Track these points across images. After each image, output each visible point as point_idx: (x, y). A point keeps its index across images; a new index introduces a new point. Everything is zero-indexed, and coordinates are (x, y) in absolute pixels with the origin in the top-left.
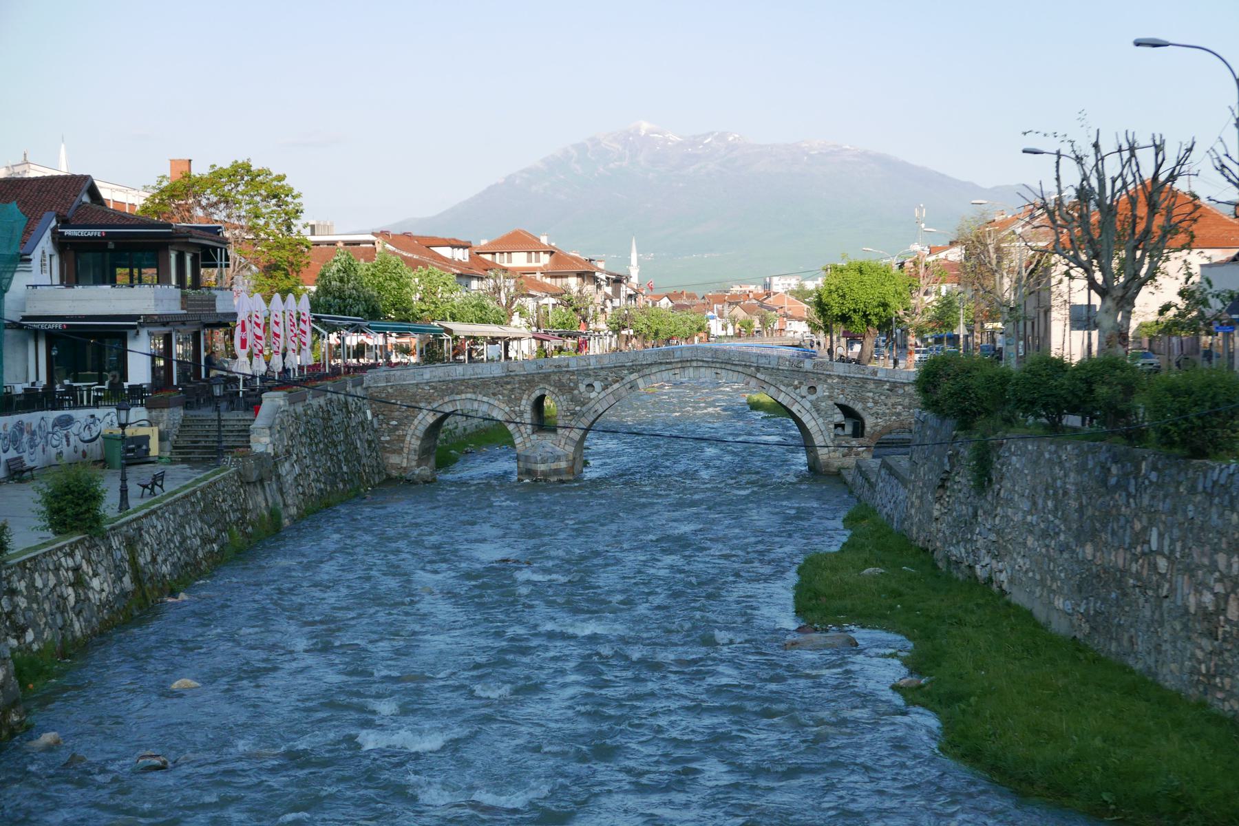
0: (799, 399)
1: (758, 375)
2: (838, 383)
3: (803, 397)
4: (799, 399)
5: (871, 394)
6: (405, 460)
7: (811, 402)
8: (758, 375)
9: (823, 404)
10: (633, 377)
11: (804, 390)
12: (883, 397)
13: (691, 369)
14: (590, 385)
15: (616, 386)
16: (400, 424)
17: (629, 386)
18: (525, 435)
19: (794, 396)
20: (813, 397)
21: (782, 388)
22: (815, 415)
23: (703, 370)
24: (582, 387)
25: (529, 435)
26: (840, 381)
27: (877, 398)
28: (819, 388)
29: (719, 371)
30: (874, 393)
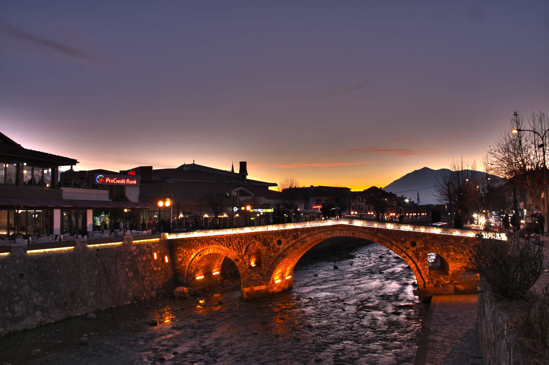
0: (405, 250)
1: (379, 235)
2: (430, 239)
3: (407, 248)
4: (405, 250)
5: (452, 246)
6: (186, 280)
7: (413, 252)
8: (379, 235)
9: (421, 253)
10: (303, 236)
11: (408, 244)
12: (460, 249)
13: (338, 231)
14: (279, 242)
15: (294, 241)
16: (183, 260)
17: (301, 241)
18: (245, 269)
19: (401, 247)
20: (415, 249)
21: (394, 242)
22: (415, 260)
23: (345, 231)
24: (275, 242)
25: (247, 269)
26: (431, 237)
27: (456, 249)
28: (418, 243)
29: (355, 232)
30: (454, 246)
